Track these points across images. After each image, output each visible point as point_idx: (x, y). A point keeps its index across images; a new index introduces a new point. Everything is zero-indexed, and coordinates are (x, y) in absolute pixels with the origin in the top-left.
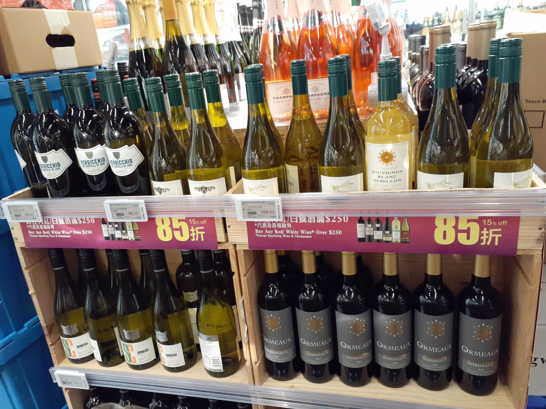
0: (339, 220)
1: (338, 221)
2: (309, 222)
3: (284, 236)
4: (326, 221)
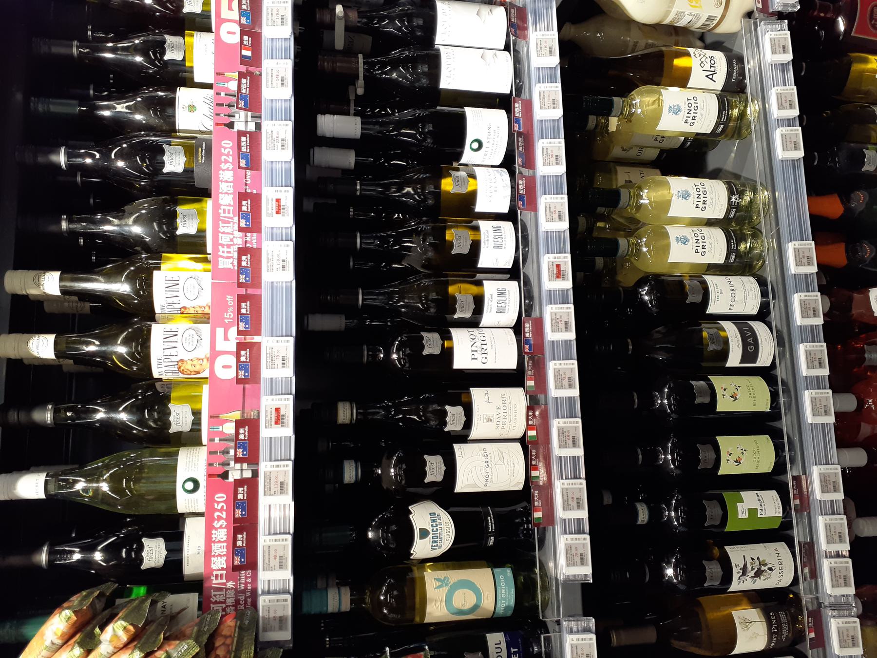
0: (223, 506)
1: (225, 508)
2: (225, 553)
4: (224, 526)
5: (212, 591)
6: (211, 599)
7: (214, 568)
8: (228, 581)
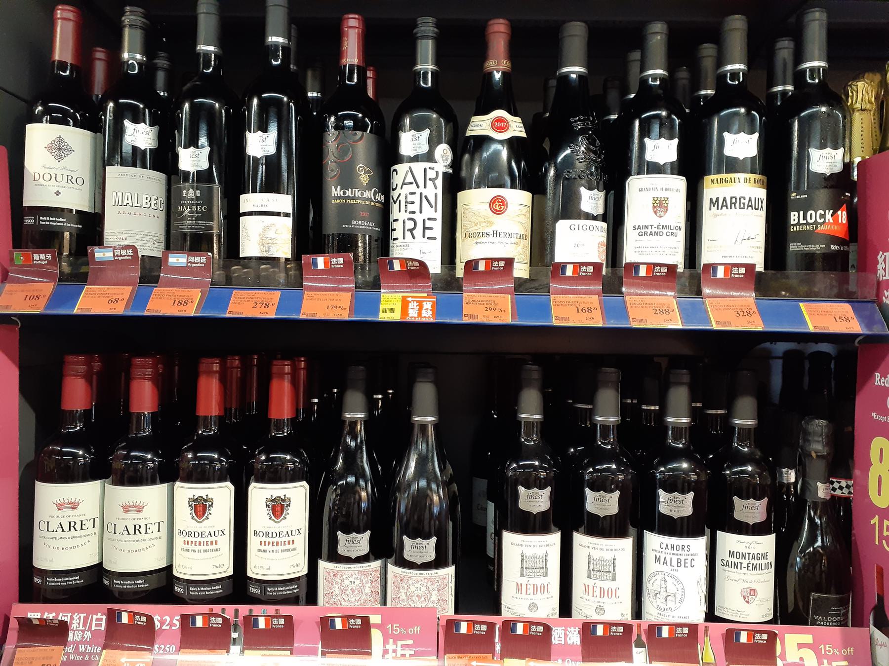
3: (72, 657)
5: (85, 615)
6: (76, 614)
8: (92, 632)
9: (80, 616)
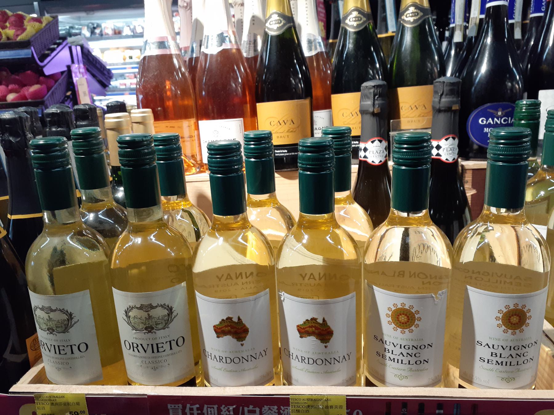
6: (223, 406)
7: (263, 409)
9: (229, 408)
